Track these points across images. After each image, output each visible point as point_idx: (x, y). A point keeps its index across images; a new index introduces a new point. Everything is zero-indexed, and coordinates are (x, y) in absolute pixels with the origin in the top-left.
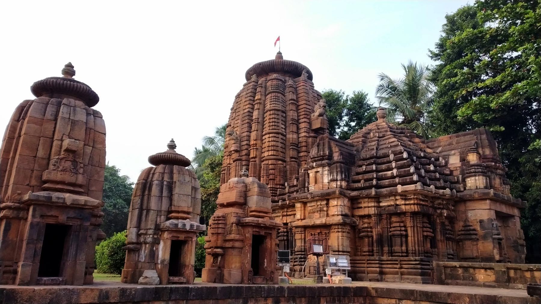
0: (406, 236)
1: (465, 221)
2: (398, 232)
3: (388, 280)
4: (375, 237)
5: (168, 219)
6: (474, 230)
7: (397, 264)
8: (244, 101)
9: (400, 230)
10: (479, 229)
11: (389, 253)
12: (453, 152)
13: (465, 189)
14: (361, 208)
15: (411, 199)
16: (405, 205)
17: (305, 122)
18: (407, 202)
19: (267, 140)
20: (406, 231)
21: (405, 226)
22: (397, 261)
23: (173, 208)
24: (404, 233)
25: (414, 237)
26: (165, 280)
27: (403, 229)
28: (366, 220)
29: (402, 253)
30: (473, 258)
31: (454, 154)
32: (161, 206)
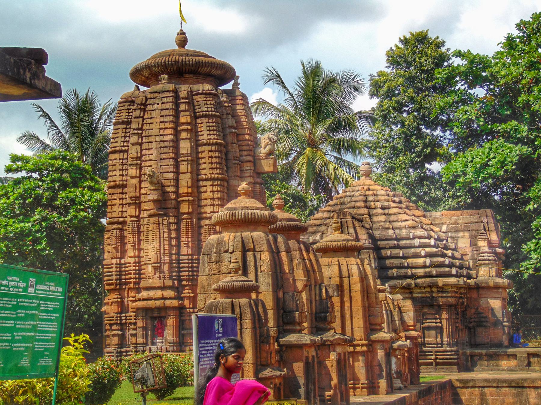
1: (477, 309)
2: (434, 325)
6: (486, 317)
8: (158, 120)
10: (490, 316)
12: (461, 234)
13: (477, 276)
15: (448, 292)
16: (442, 297)
17: (250, 161)
18: (445, 295)
19: (210, 189)
22: (432, 352)
25: (449, 328)
30: (484, 345)
31: (463, 237)
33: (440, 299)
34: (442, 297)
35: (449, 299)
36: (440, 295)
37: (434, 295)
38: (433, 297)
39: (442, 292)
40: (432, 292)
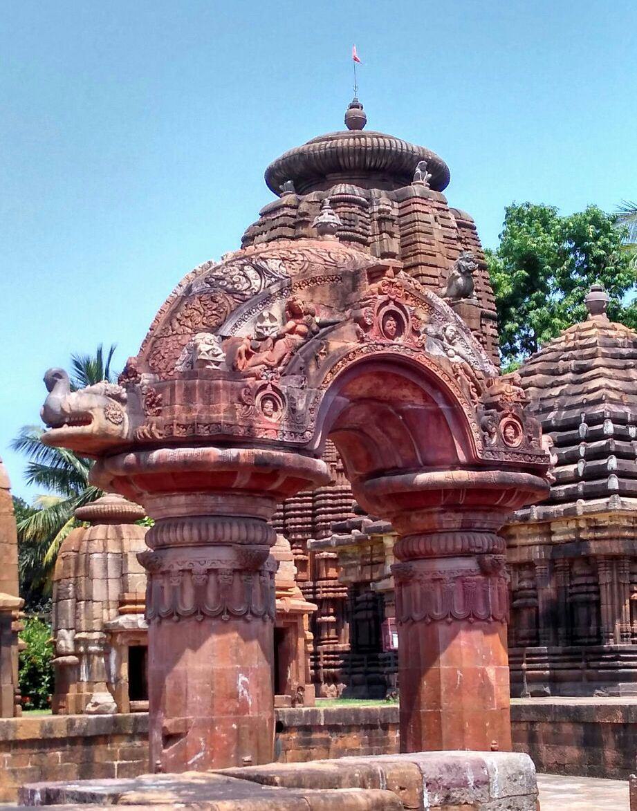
0: (598, 603)
2: (582, 596)
3: (565, 692)
4: (540, 607)
5: (121, 613)
7: (580, 661)
9: (587, 593)
11: (567, 638)
14: (515, 546)
15: (605, 528)
16: (596, 539)
18: (599, 535)
20: (598, 592)
21: (596, 584)
23: (127, 597)
24: (594, 597)
26: (125, 707)
27: (593, 588)
28: (525, 573)
29: (590, 637)
32: (108, 594)
33: (592, 544)
34: (596, 539)
35: (607, 543)
36: (591, 535)
37: (582, 536)
38: (582, 540)
39: (597, 529)
40: (580, 529)
